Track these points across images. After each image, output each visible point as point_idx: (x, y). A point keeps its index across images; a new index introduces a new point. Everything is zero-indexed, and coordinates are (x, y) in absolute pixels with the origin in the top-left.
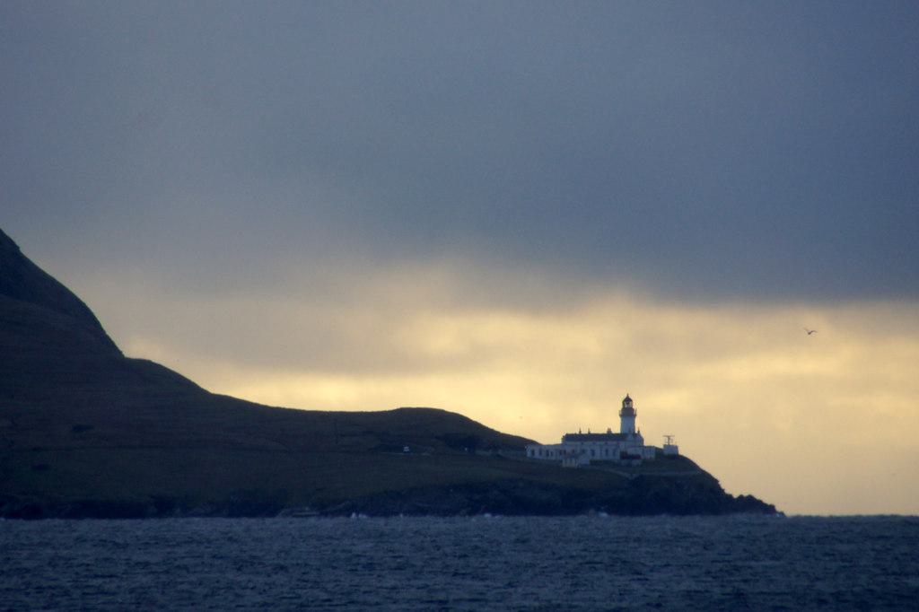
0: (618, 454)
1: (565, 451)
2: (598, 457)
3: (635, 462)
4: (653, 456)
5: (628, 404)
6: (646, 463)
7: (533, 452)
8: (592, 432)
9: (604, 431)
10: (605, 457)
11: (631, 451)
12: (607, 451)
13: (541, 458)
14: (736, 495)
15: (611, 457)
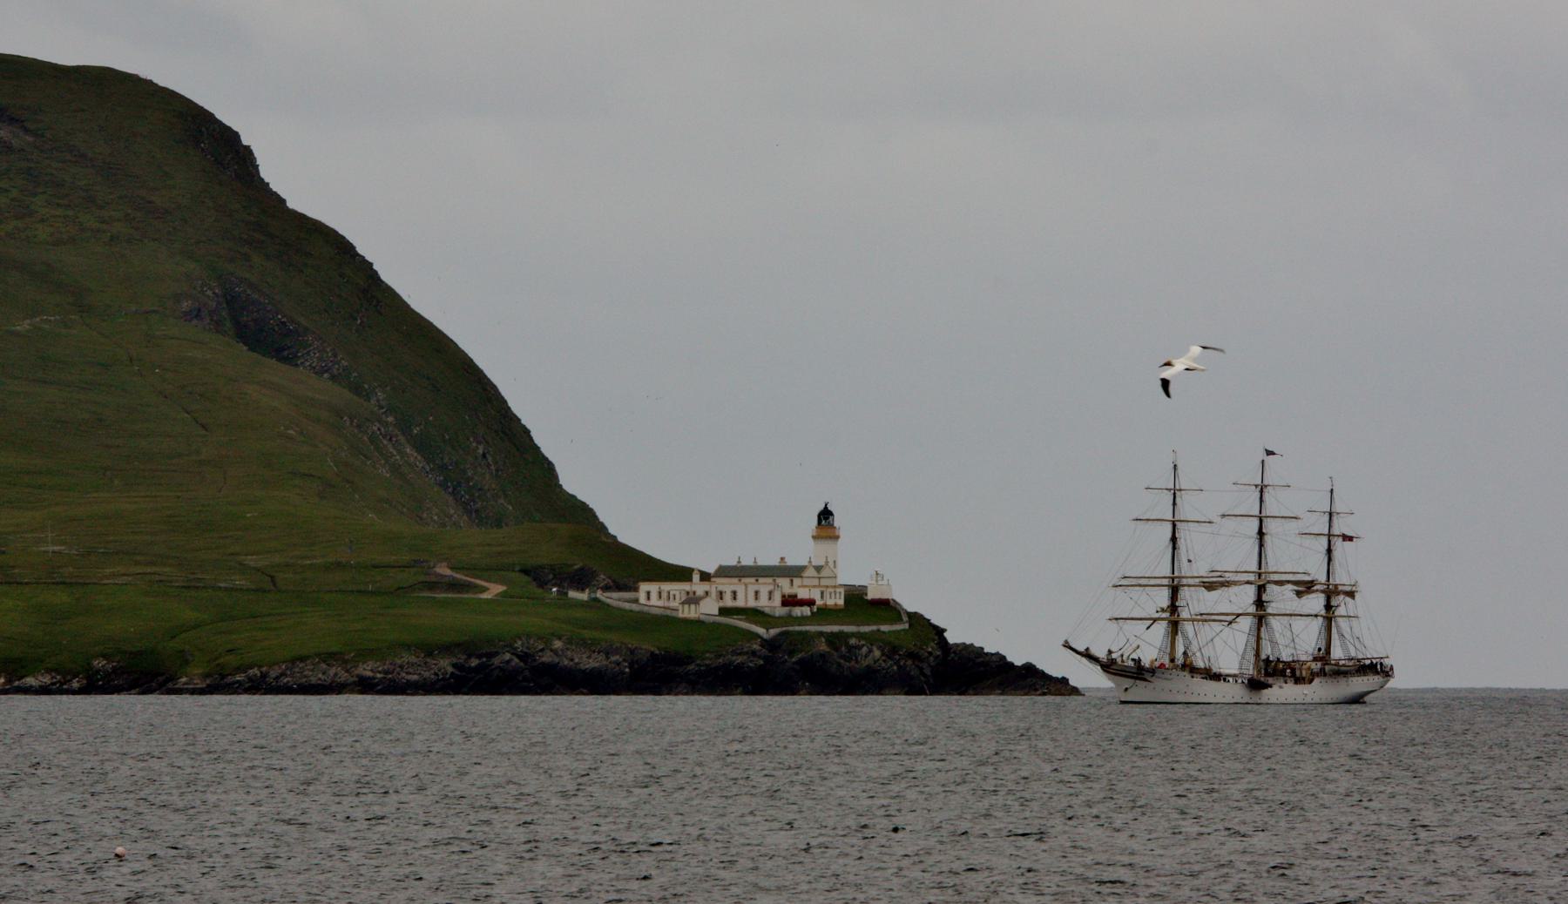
0: (777, 600)
1: (694, 593)
2: (740, 603)
3: (798, 611)
4: (841, 602)
5: (826, 519)
6: (825, 614)
7: (648, 593)
8: (760, 563)
9: (775, 562)
10: (752, 603)
11: (803, 594)
12: (757, 593)
13: (660, 603)
14: (1018, 662)
15: (763, 603)
